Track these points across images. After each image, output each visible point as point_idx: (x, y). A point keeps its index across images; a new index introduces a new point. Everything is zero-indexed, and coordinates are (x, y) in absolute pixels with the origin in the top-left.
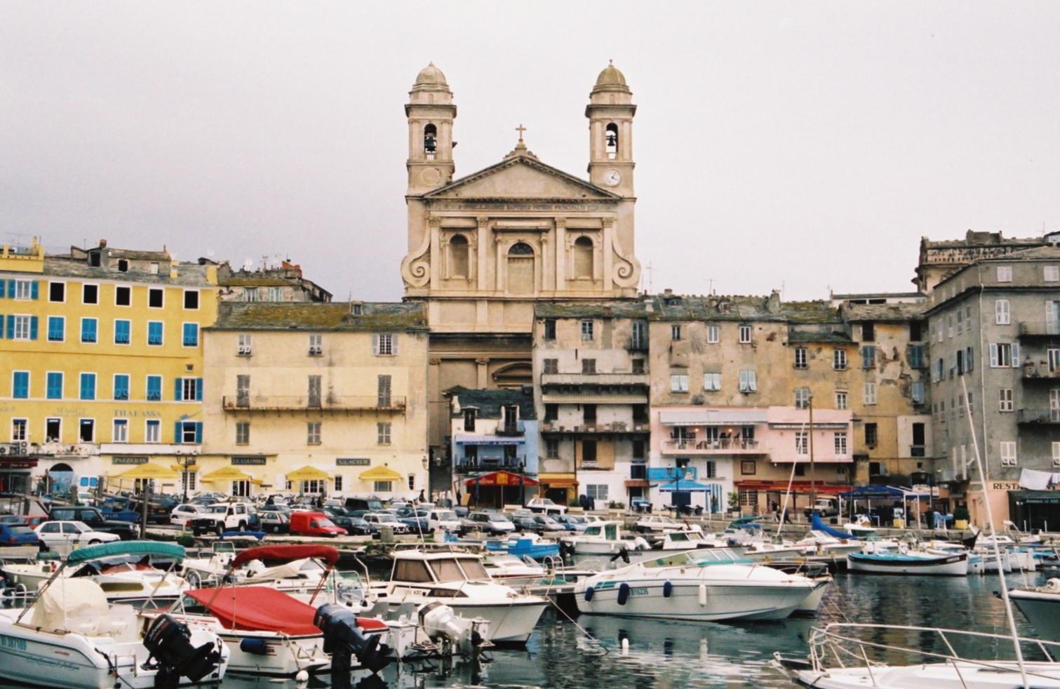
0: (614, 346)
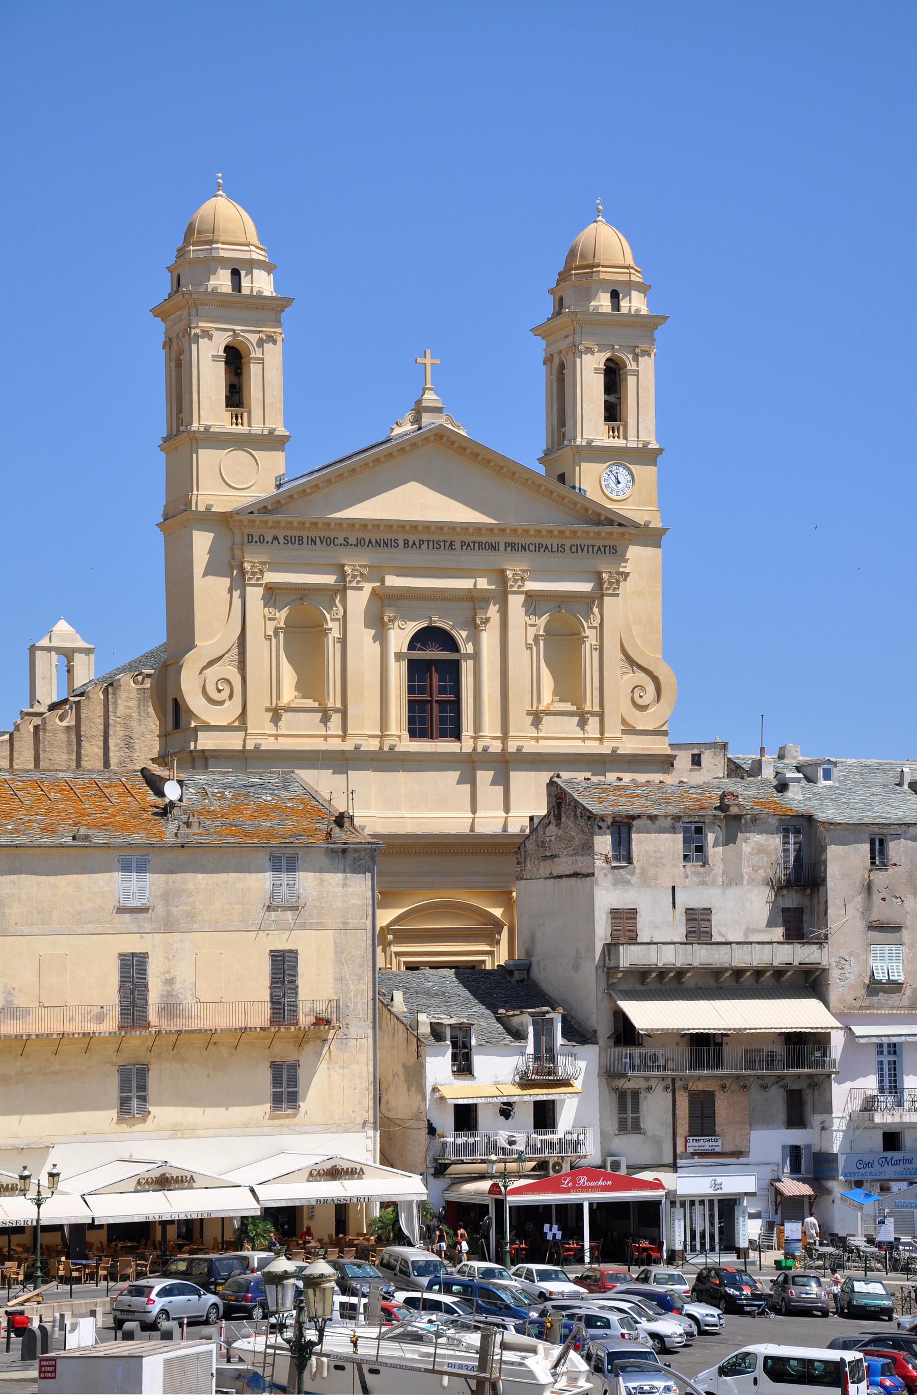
0: (746, 877)
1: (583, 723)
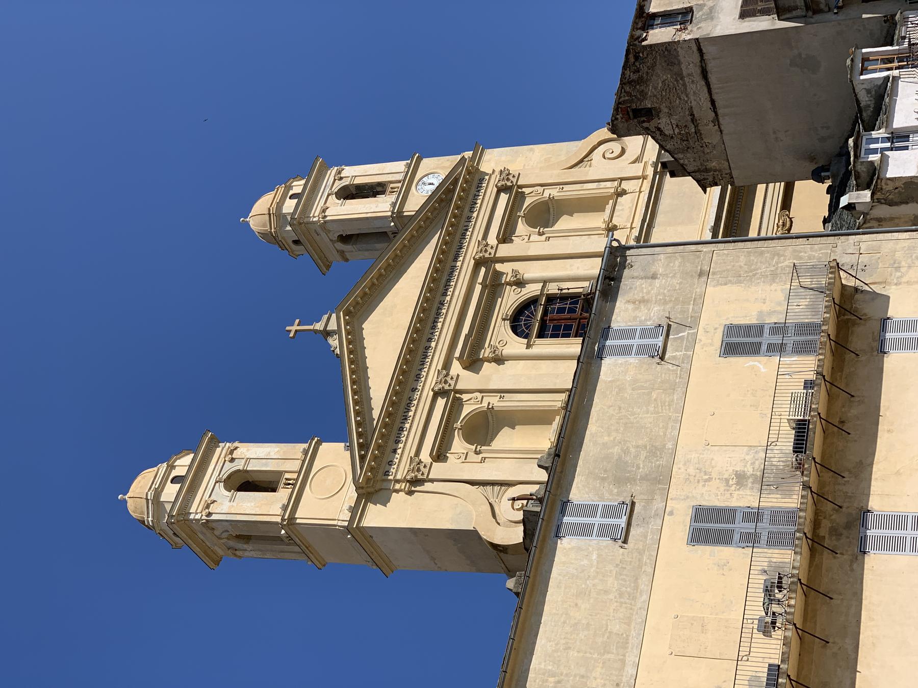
1: (624, 193)
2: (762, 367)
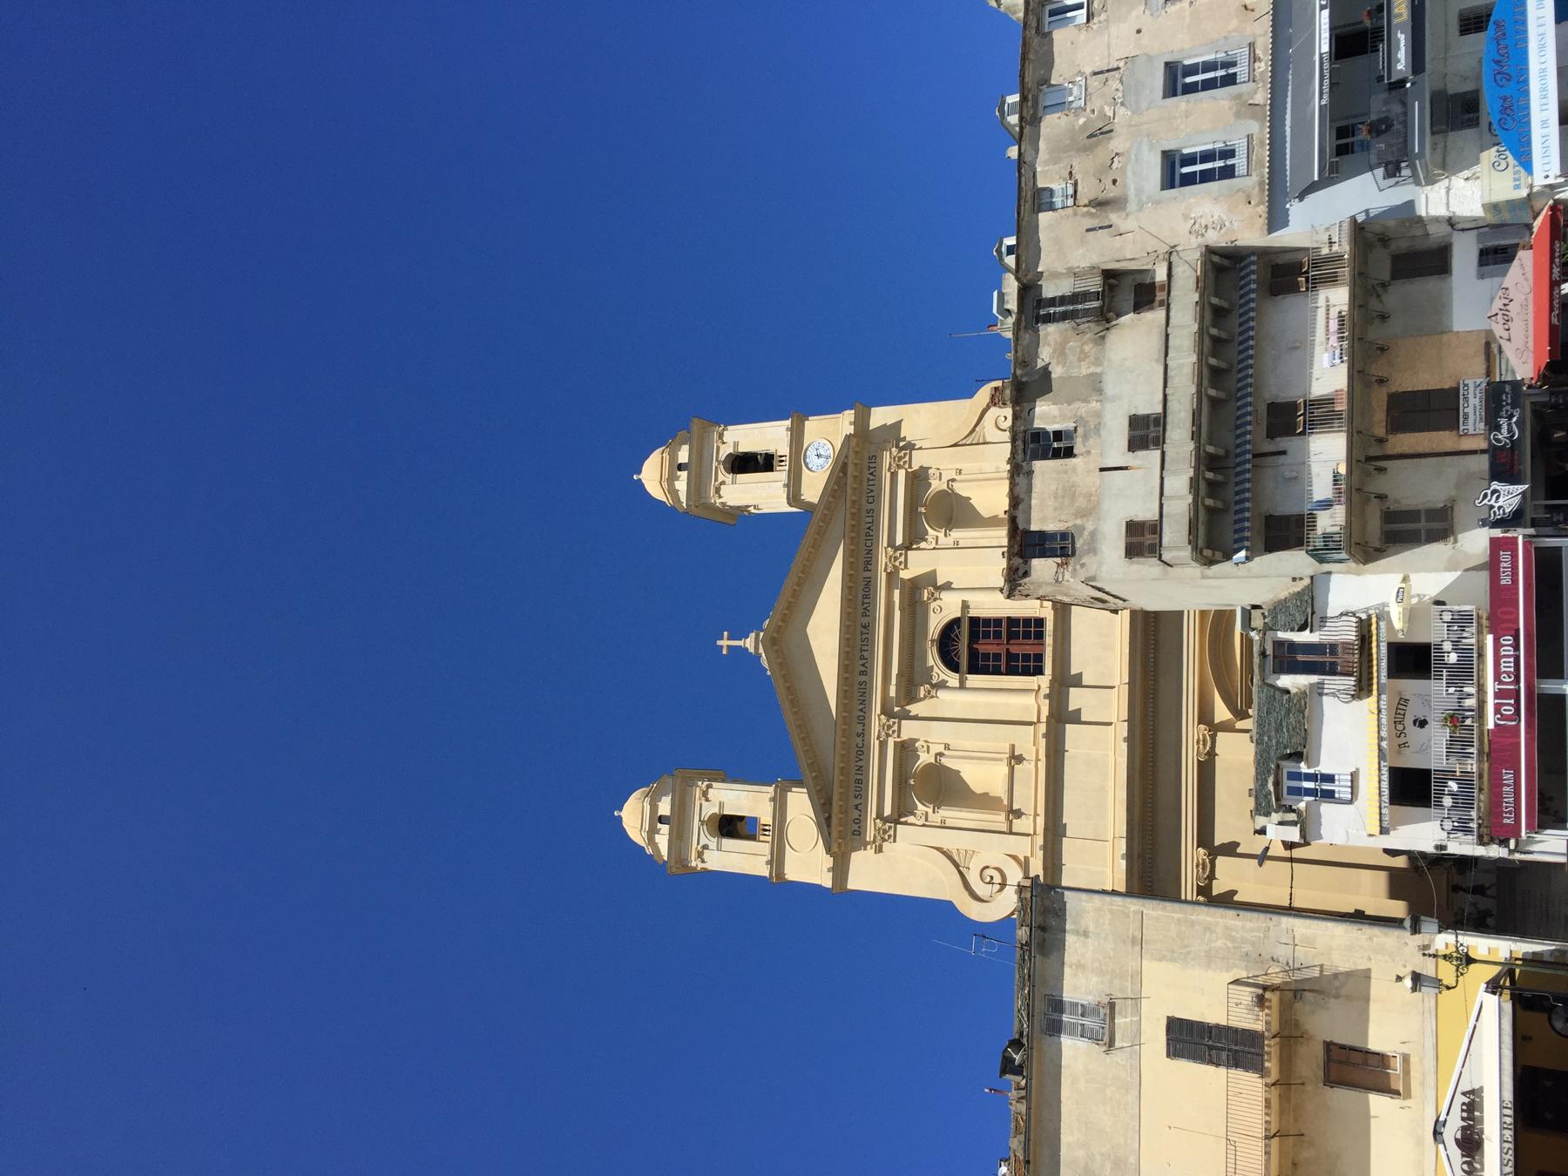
0: (1093, 369)
2: (1210, 1081)
